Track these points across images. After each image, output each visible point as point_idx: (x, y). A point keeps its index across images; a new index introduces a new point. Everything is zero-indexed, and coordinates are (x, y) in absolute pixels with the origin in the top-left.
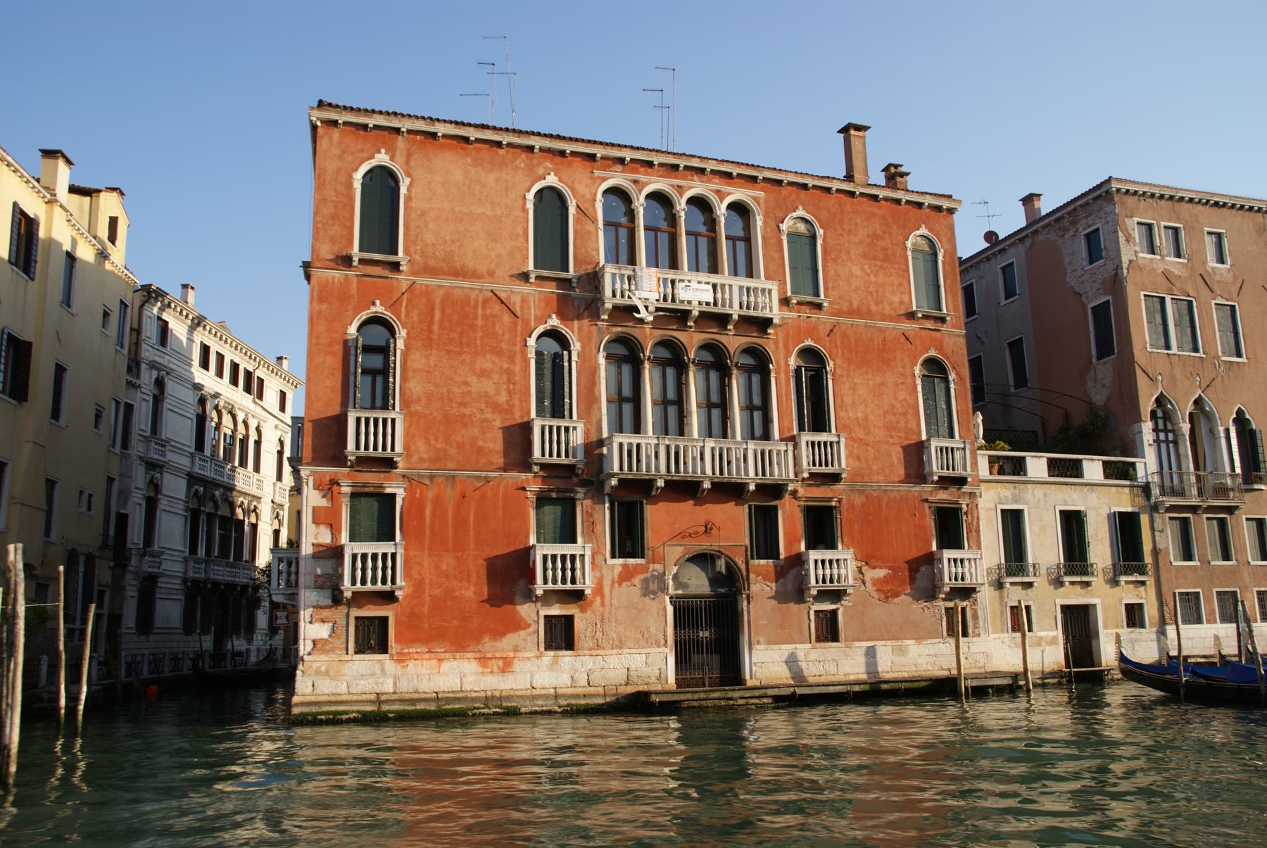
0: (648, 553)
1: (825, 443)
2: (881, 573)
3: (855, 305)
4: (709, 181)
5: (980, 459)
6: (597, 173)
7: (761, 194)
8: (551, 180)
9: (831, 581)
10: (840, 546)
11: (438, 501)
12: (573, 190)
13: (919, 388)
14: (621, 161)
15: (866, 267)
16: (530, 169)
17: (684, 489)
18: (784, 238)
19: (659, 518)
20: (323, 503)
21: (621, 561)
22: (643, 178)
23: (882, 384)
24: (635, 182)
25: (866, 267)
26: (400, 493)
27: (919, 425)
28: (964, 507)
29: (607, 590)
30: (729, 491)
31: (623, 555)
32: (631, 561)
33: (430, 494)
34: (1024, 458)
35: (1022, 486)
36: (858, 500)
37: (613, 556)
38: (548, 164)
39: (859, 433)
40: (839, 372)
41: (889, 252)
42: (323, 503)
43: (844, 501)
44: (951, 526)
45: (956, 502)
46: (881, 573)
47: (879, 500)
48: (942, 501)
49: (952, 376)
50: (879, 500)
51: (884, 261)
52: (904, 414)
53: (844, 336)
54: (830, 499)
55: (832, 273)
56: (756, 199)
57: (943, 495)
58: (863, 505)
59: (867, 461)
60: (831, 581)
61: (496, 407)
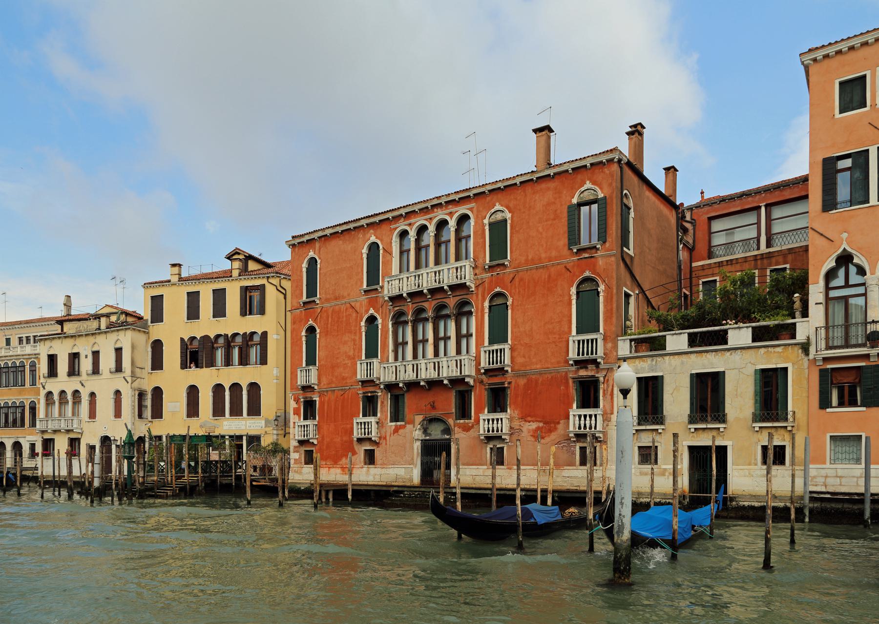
0: (407, 419)
1: (497, 350)
2: (534, 426)
3: (530, 257)
4: (447, 209)
5: (620, 344)
6: (392, 227)
7: (473, 205)
8: (373, 239)
9: (493, 431)
10: (509, 410)
11: (329, 399)
12: (381, 241)
13: (574, 302)
14: (401, 215)
15: (540, 229)
16: (364, 235)
17: (412, 385)
18: (487, 228)
19: (409, 401)
20: (296, 406)
21: (394, 424)
22: (412, 221)
23: (545, 305)
24: (410, 224)
25: (540, 229)
26: (317, 399)
27: (570, 328)
28: (601, 379)
29: (388, 438)
30: (434, 384)
31: (397, 421)
32: (399, 423)
33: (327, 399)
34: (665, 336)
35: (659, 359)
36: (522, 382)
37: (391, 421)
38: (372, 231)
39: (527, 340)
40: (515, 304)
41: (559, 211)
42: (296, 406)
43: (513, 384)
44: (589, 394)
45: (593, 376)
46: (534, 426)
47: (537, 381)
48: (582, 377)
49: (602, 288)
50: (537, 381)
51: (554, 219)
52: (560, 322)
53: (521, 280)
54: (503, 383)
55: (516, 240)
56: (471, 209)
57: (583, 373)
58: (525, 385)
59: (529, 357)
60: (493, 431)
61: (349, 357)
